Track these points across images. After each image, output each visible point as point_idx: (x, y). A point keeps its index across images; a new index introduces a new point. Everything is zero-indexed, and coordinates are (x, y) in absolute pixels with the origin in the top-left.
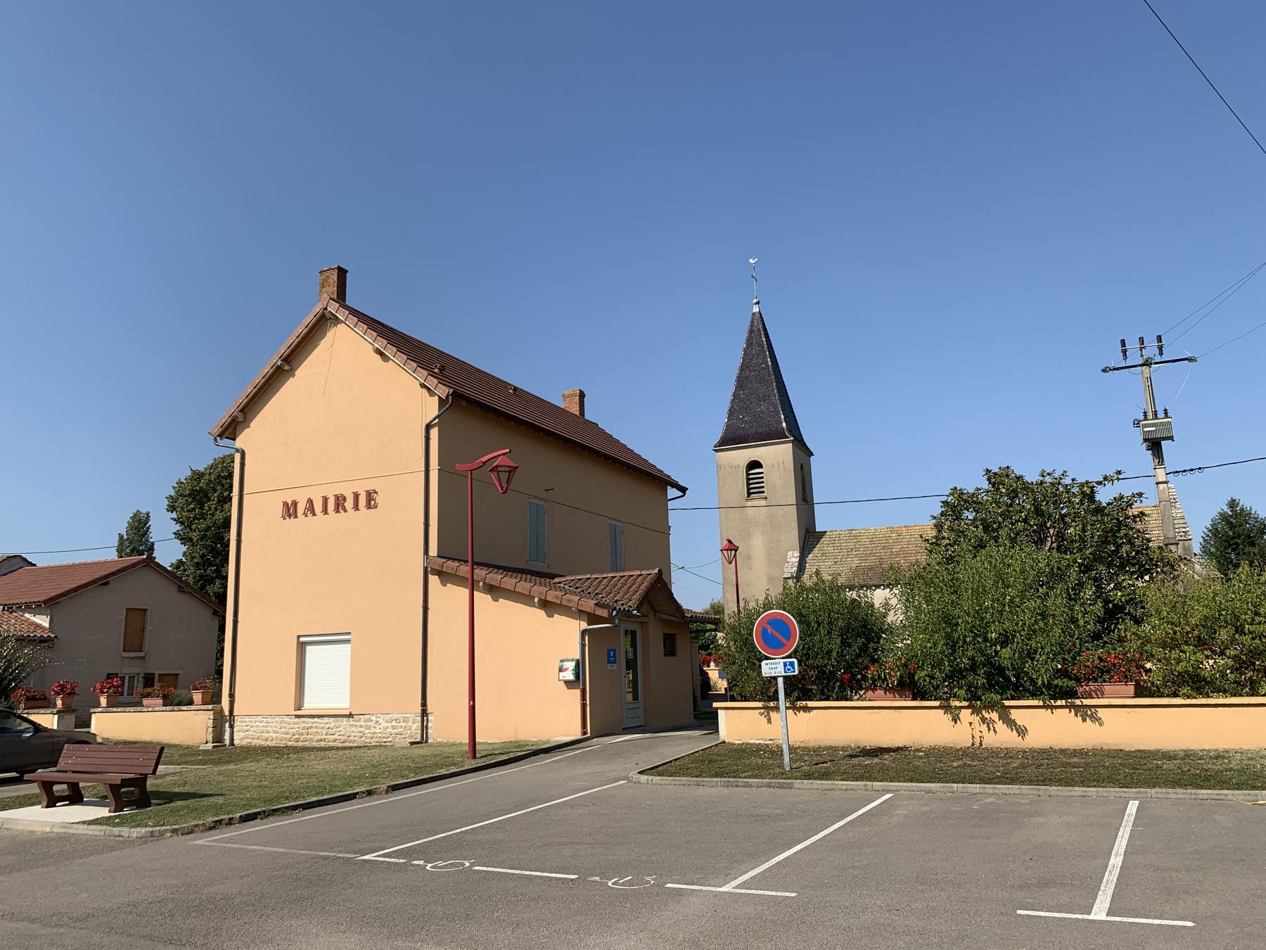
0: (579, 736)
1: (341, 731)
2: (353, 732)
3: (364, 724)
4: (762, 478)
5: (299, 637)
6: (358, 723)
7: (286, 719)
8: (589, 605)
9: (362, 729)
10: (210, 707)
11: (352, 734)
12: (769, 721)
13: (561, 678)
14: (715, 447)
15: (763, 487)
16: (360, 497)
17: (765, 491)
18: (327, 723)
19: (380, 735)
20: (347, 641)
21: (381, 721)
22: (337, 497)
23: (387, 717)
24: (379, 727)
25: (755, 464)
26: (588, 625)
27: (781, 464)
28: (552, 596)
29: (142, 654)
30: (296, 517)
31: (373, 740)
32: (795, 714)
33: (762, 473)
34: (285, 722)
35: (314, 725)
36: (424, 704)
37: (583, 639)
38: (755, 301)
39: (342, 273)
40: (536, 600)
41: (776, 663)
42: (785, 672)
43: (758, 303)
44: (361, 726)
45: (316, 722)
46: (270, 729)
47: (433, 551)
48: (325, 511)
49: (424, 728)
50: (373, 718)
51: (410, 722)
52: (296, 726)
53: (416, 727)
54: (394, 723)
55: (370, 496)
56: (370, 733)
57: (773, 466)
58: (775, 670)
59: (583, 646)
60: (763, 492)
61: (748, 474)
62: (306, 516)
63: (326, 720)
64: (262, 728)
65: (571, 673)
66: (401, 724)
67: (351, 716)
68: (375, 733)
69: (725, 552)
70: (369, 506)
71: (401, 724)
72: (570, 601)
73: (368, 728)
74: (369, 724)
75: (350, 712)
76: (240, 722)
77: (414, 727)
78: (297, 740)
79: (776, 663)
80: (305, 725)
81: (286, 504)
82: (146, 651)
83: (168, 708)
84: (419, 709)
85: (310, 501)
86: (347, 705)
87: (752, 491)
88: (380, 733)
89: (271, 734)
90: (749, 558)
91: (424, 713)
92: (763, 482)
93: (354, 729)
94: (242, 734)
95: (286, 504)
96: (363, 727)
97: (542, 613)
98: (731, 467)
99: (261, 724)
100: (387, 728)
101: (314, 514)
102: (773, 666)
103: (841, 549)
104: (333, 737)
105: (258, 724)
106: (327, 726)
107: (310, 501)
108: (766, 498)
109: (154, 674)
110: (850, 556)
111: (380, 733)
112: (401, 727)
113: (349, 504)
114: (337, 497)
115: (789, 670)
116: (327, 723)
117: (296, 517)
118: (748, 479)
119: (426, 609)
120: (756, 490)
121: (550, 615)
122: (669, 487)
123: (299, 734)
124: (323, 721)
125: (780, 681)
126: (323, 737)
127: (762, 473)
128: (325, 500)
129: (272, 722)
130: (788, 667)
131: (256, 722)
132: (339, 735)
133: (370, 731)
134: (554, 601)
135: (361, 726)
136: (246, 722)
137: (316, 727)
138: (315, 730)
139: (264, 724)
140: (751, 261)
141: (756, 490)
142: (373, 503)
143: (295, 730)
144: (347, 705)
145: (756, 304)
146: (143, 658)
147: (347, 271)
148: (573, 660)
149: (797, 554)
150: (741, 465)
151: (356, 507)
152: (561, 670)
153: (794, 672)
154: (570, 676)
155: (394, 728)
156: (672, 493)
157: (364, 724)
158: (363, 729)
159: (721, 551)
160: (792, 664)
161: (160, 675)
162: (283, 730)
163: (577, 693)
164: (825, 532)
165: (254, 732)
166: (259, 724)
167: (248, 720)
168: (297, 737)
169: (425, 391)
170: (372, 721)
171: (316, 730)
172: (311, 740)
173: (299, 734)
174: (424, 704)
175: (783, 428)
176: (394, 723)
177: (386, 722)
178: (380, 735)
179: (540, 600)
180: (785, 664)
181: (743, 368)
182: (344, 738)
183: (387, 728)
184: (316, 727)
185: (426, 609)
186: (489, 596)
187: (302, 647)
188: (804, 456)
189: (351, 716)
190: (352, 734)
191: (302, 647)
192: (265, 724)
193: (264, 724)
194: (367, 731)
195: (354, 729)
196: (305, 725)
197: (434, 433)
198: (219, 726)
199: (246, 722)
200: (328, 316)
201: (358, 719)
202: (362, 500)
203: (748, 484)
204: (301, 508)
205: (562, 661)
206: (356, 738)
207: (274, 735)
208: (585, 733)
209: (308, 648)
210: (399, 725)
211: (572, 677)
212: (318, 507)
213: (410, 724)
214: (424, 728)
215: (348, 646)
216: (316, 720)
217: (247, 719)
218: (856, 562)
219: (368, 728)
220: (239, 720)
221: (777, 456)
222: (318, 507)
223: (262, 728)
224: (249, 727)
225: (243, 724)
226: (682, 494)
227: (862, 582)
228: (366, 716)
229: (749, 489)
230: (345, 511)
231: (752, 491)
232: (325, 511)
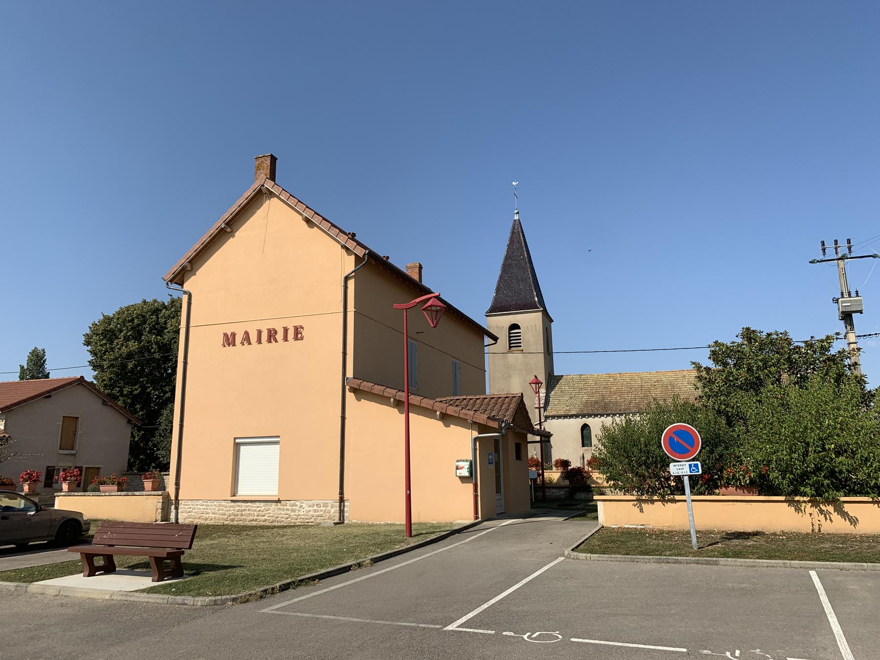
0: (470, 520)
1: (270, 513)
2: (280, 514)
3: (290, 508)
4: (520, 336)
5: (235, 439)
6: (285, 507)
7: (223, 503)
8: (482, 418)
9: (288, 512)
10: (160, 493)
11: (280, 516)
12: (641, 511)
13: (458, 474)
14: (486, 313)
15: (520, 343)
16: (263, 334)
17: (522, 345)
18: (258, 507)
19: (303, 517)
20: (277, 443)
21: (304, 505)
22: (269, 331)
24: (303, 510)
25: (515, 326)
26: (479, 434)
27: (533, 327)
28: (451, 410)
29: (74, 452)
30: (234, 345)
31: (298, 520)
32: (664, 505)
33: (520, 333)
34: (222, 506)
35: (247, 508)
36: (342, 493)
37: (475, 445)
38: (516, 211)
39: (273, 159)
40: (438, 413)
41: (683, 465)
42: (691, 472)
43: (518, 213)
44: (287, 510)
45: (249, 506)
46: (209, 511)
47: (350, 374)
48: (259, 341)
49: (342, 512)
50: (298, 503)
51: (329, 507)
52: (232, 509)
53: (334, 511)
54: (315, 508)
55: (298, 331)
56: (295, 515)
57: (528, 328)
58: (682, 471)
59: (475, 449)
60: (520, 346)
61: (510, 333)
62: (243, 345)
63: (257, 504)
64: (202, 510)
65: (466, 470)
66: (321, 508)
67: (279, 501)
68: (299, 515)
69: (533, 385)
70: (296, 338)
71: (321, 508)
72: (466, 414)
73: (294, 511)
74: (294, 508)
75: (279, 498)
76: (184, 505)
77: (333, 510)
78: (233, 520)
79: (683, 465)
80: (240, 508)
81: (225, 335)
82: (77, 449)
83: (123, 493)
84: (338, 497)
85: (247, 333)
86: (276, 493)
87: (512, 345)
88: (303, 515)
89: (210, 515)
91: (342, 500)
92: (520, 339)
93: (281, 512)
94: (185, 515)
95: (225, 335)
96: (289, 511)
97: (440, 424)
99: (202, 507)
100: (310, 511)
101: (250, 344)
102: (680, 467)
103: (574, 388)
104: (263, 518)
105: (199, 506)
106: (259, 509)
107: (247, 333)
109: (82, 467)
110: (581, 393)
111: (303, 515)
112: (322, 511)
113: (280, 336)
114: (269, 331)
115: (694, 470)
116: (258, 507)
117: (234, 345)
118: (510, 337)
120: (515, 345)
121: (447, 425)
123: (234, 515)
124: (255, 505)
125: (686, 480)
126: (255, 518)
127: (520, 333)
128: (260, 333)
129: (212, 505)
130: (693, 468)
131: (197, 505)
132: (269, 517)
133: (295, 513)
134: (453, 414)
135: (287, 510)
136: (189, 505)
137: (249, 510)
138: (248, 512)
139: (204, 507)
140: (514, 183)
141: (515, 345)
142: (299, 336)
143: (231, 512)
144: (276, 493)
145: (516, 214)
146: (74, 455)
147: (277, 159)
148: (467, 461)
150: (505, 327)
151: (286, 339)
152: (457, 468)
153: (698, 472)
154: (465, 473)
155: (315, 511)
156: (487, 340)
157: (290, 508)
158: (289, 512)
159: (530, 384)
160: (696, 466)
161: (86, 468)
162: (221, 512)
163: (470, 486)
164: (563, 376)
165: (196, 513)
166: (199, 506)
167: (190, 503)
168: (232, 517)
169: (344, 251)
170: (296, 505)
171: (249, 512)
172: (245, 520)
173: (234, 515)
174: (342, 493)
175: (535, 301)
176: (315, 508)
177: (309, 506)
178: (303, 517)
179: (441, 413)
180: (690, 465)
181: (507, 258)
182: (273, 518)
183: (310, 511)
184: (249, 510)
186: (396, 410)
187: (237, 446)
188: (548, 322)
189: (279, 501)
190: (280, 516)
191: (237, 446)
192: (205, 507)
193: (204, 507)
194: (292, 514)
195: (281, 512)
196: (240, 508)
197: (351, 284)
198: (166, 508)
199: (189, 505)
200: (264, 191)
201: (285, 504)
203: (510, 340)
204: (239, 339)
205: (457, 461)
206: (283, 519)
207: (213, 516)
208: (477, 518)
209: (242, 448)
210: (319, 509)
211: (467, 474)
212: (253, 338)
213: (329, 508)
214: (342, 512)
215: (277, 447)
216: (249, 504)
217: (190, 502)
218: (586, 397)
219: (294, 511)
220: (183, 503)
221: (530, 321)
222: (253, 338)
223: (202, 510)
224: (191, 509)
225: (187, 507)
226: (494, 342)
227: (590, 412)
228: (292, 502)
229: (510, 344)
230: (276, 341)
231: (512, 345)
232: (259, 341)
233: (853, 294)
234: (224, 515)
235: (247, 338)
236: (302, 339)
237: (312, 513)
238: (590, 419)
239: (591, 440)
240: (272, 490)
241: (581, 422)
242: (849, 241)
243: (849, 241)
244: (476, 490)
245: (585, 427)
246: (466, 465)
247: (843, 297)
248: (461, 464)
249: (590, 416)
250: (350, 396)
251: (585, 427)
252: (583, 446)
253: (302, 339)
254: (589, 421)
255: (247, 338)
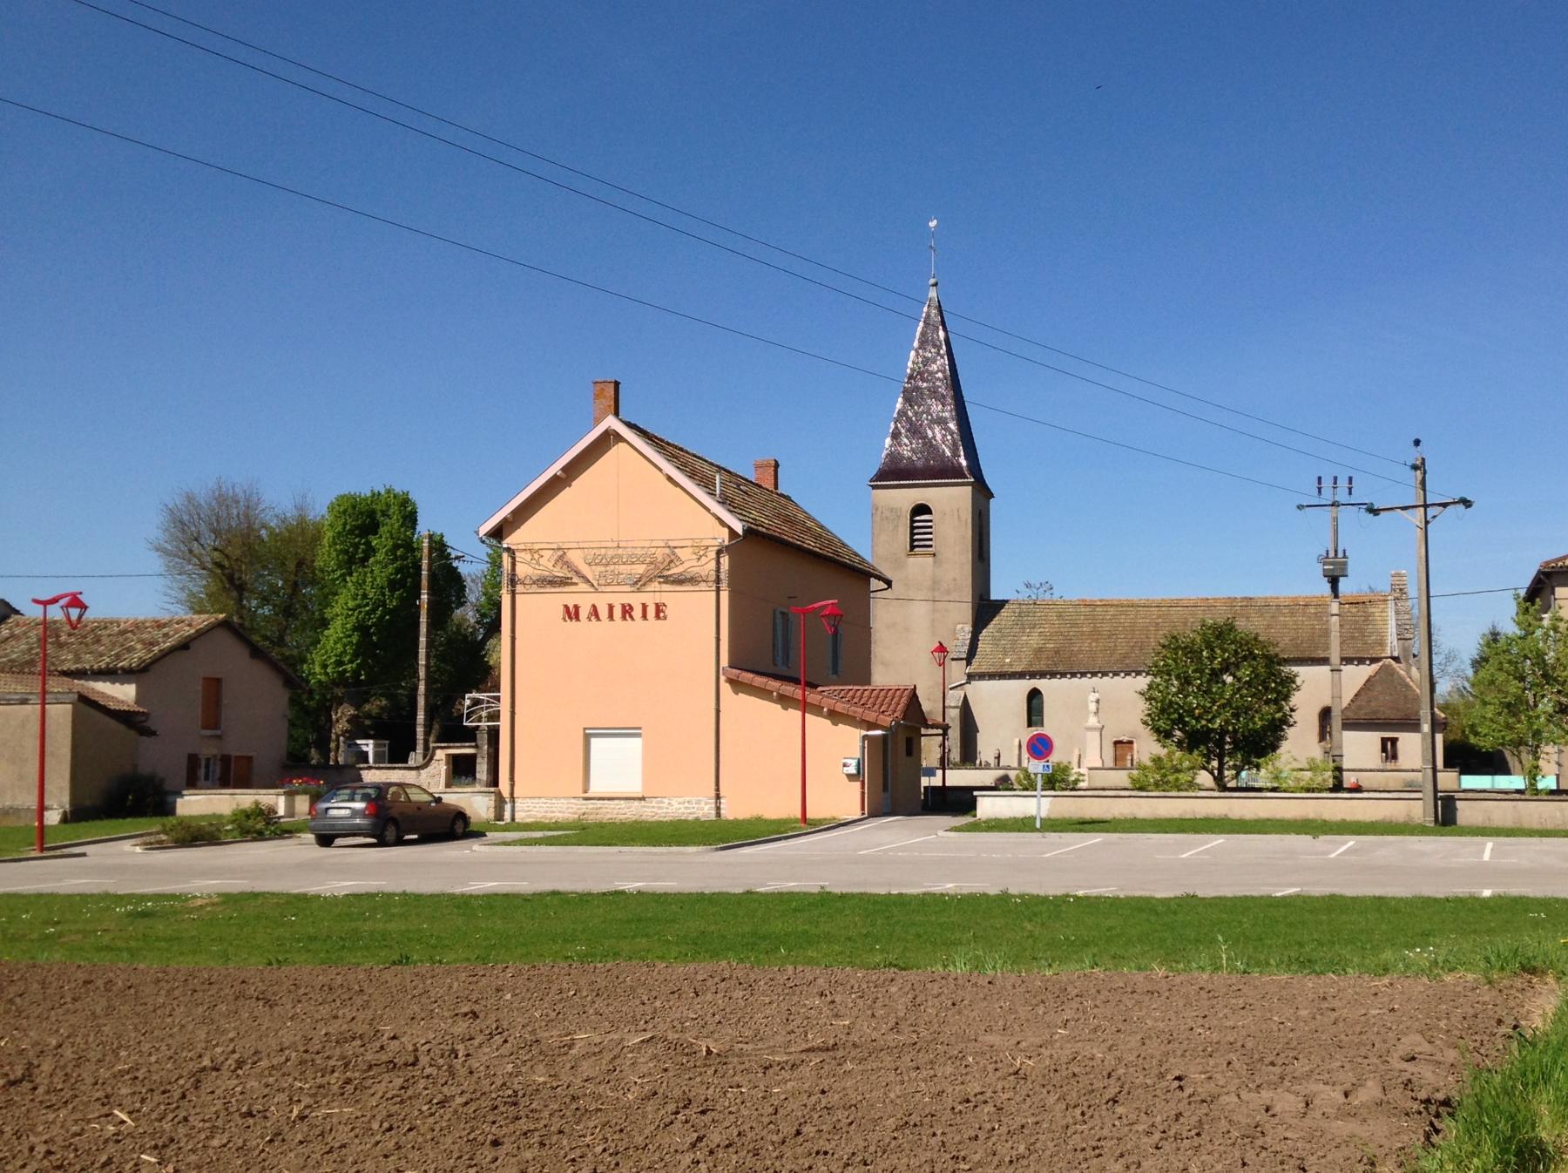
4: (931, 527)
5: (585, 729)
7: (573, 801)
14: (871, 481)
20: (638, 735)
21: (673, 802)
22: (623, 606)
23: (681, 800)
25: (921, 509)
28: (840, 707)
30: (577, 618)
33: (931, 521)
36: (718, 790)
37: (863, 743)
38: (932, 281)
39: (617, 384)
40: (825, 710)
43: (936, 285)
44: (653, 807)
47: (724, 662)
48: (611, 617)
49: (718, 809)
50: (666, 801)
54: (686, 805)
55: (659, 609)
59: (864, 747)
60: (931, 546)
61: (912, 521)
62: (590, 620)
63: (616, 802)
67: (643, 799)
69: (936, 654)
70: (658, 617)
72: (855, 712)
73: (660, 808)
77: (707, 807)
81: (566, 607)
84: (713, 793)
87: (916, 543)
90: (907, 630)
91: (718, 797)
94: (523, 814)
95: (566, 607)
97: (828, 722)
98: (892, 510)
108: (934, 555)
113: (637, 613)
114: (623, 606)
118: (912, 528)
119: (718, 711)
121: (835, 724)
122: (872, 579)
127: (931, 521)
128: (611, 607)
135: (653, 807)
138: (605, 810)
142: (662, 615)
145: (933, 285)
149: (968, 628)
150: (904, 509)
151: (644, 616)
152: (845, 765)
154: (853, 770)
155: (686, 808)
163: (857, 785)
164: (1007, 601)
174: (718, 790)
175: (960, 464)
176: (686, 805)
179: (829, 710)
185: (718, 711)
186: (779, 706)
187: (587, 738)
189: (643, 799)
191: (587, 738)
194: (659, 811)
197: (725, 560)
202: (651, 611)
203: (912, 534)
204: (584, 613)
209: (593, 740)
211: (854, 772)
212: (603, 613)
213: (702, 805)
214: (718, 809)
215: (637, 742)
216: (606, 802)
217: (528, 800)
219: (660, 808)
221: (950, 501)
222: (603, 613)
227: (1044, 668)
229: (912, 541)
230: (631, 617)
231: (916, 543)
233: (1340, 554)
234: (575, 813)
235: (595, 612)
236: (665, 618)
237: (682, 810)
238: (1043, 681)
239: (1042, 716)
240: (636, 788)
241: (1027, 685)
242: (1350, 479)
243: (1350, 479)
244: (863, 787)
245: (1034, 695)
246: (854, 763)
247: (1327, 557)
248: (849, 761)
249: (1042, 675)
250: (726, 688)
251: (1034, 695)
252: (1030, 725)
253: (665, 618)
254: (1040, 684)
255: (595, 612)
